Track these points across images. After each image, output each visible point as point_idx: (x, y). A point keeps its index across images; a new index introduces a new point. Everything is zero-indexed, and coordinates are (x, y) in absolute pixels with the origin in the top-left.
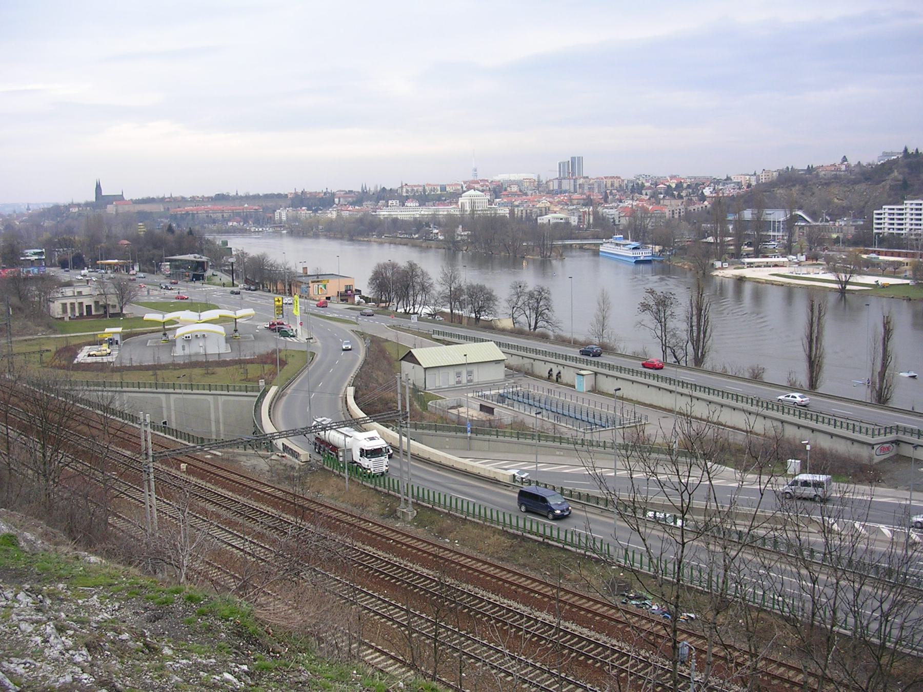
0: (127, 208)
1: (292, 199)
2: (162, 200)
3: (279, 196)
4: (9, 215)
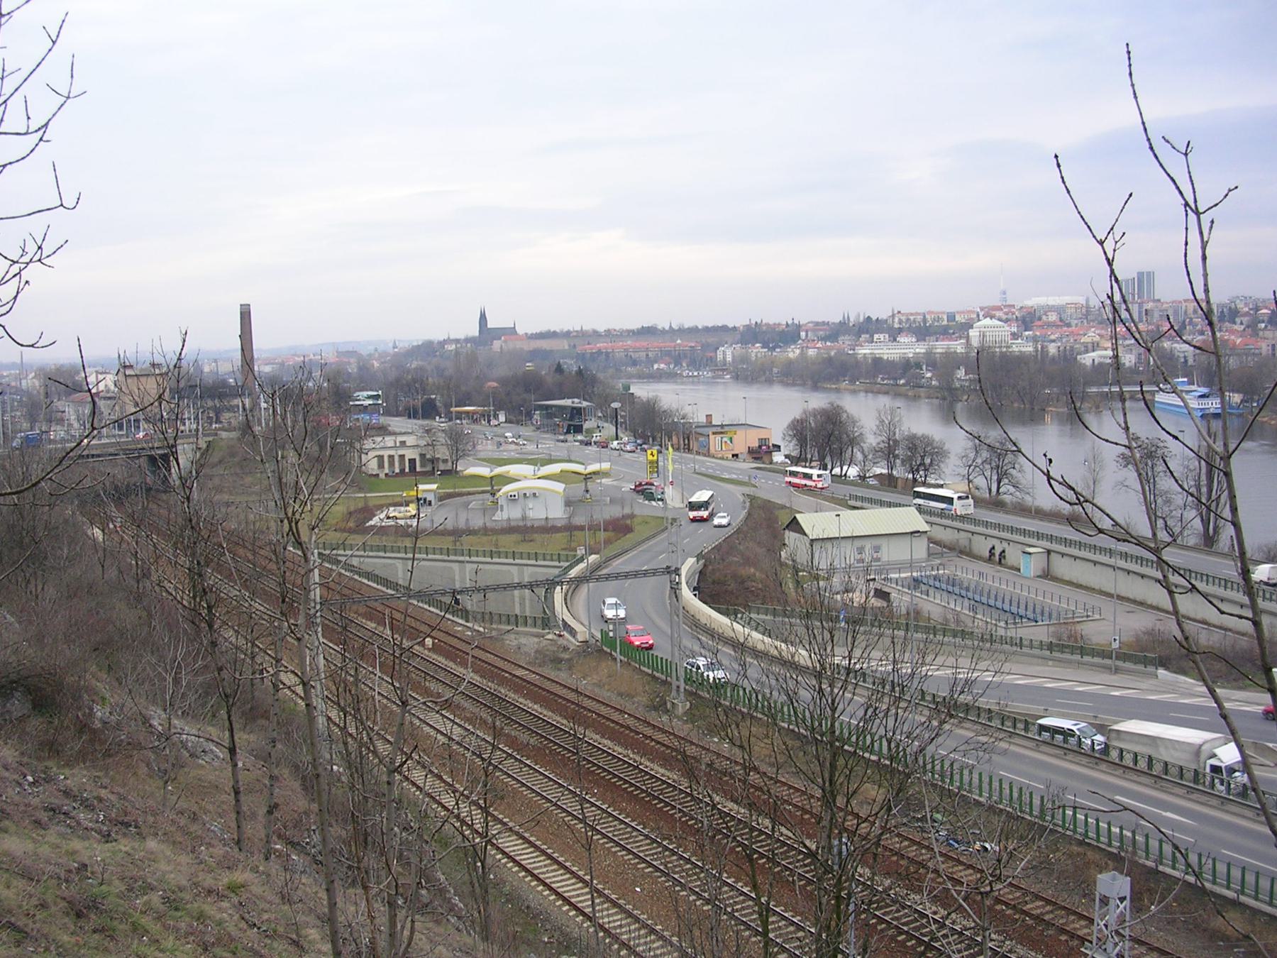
0: (519, 345)
1: (742, 334)
2: (567, 334)
3: (724, 328)
4: (370, 355)
